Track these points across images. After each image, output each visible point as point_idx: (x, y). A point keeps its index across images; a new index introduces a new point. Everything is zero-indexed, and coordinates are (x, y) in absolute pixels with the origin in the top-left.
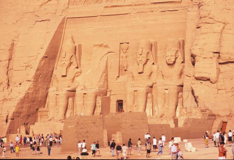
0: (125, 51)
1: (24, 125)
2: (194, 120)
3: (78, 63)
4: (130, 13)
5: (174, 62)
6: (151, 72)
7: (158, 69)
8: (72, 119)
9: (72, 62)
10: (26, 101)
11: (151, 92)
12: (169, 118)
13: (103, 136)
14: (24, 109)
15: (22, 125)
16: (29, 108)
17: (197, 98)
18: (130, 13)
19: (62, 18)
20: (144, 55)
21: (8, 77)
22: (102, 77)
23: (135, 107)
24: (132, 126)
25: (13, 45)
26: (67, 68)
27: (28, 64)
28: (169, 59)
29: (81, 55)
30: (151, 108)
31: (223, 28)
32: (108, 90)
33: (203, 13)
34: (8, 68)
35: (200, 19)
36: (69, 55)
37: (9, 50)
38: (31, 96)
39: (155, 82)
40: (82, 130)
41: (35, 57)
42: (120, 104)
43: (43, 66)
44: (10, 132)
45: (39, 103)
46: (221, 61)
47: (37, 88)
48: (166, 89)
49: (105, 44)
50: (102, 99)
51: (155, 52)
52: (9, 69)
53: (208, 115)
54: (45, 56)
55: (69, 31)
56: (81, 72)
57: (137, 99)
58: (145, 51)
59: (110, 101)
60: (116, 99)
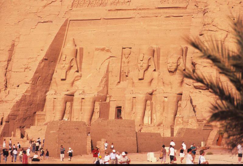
0: (126, 56)
1: (20, 128)
2: (188, 130)
3: (79, 66)
4: (134, 18)
6: (151, 79)
7: (159, 77)
8: (54, 124)
9: (72, 65)
10: (23, 103)
11: (151, 99)
12: (167, 126)
13: (86, 143)
14: (20, 112)
15: (18, 128)
16: (26, 111)
17: (195, 107)
18: (134, 18)
19: (64, 20)
20: (145, 61)
21: (6, 79)
22: (101, 82)
24: (118, 133)
25: (13, 45)
26: (67, 72)
27: (27, 66)
28: (171, 66)
29: (82, 59)
30: (150, 116)
31: (225, 36)
32: (108, 96)
33: (207, 20)
35: (204, 26)
36: (69, 58)
37: (9, 51)
38: (28, 99)
39: (155, 89)
40: (64, 135)
41: (34, 59)
42: (119, 110)
43: (43, 69)
44: (5, 135)
45: (37, 106)
47: (35, 91)
48: (165, 97)
50: (101, 105)
51: (157, 58)
52: (7, 70)
53: (204, 125)
54: (44, 58)
55: (71, 33)
57: (135, 106)
58: (147, 57)
59: (109, 108)
60: (115, 105)
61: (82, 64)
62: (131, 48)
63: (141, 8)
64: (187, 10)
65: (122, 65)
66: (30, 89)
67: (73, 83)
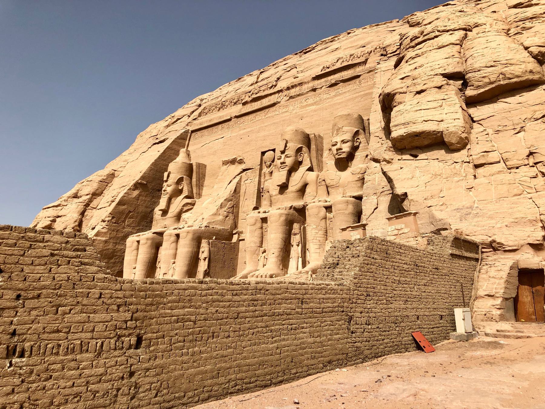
3: (195, 191)
4: (279, 102)
5: (351, 156)
9: (180, 188)
17: (403, 200)
18: (279, 102)
20: (290, 152)
23: (263, 253)
30: (300, 255)
34: (87, 205)
43: (138, 200)
46: (470, 92)
47: (121, 235)
49: (239, 159)
56: (193, 205)
58: (293, 146)
61: (202, 189)
62: (274, 150)
63: (290, 86)
64: (368, 65)
65: (262, 180)
66: (107, 230)
67: (178, 217)
